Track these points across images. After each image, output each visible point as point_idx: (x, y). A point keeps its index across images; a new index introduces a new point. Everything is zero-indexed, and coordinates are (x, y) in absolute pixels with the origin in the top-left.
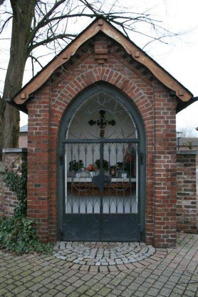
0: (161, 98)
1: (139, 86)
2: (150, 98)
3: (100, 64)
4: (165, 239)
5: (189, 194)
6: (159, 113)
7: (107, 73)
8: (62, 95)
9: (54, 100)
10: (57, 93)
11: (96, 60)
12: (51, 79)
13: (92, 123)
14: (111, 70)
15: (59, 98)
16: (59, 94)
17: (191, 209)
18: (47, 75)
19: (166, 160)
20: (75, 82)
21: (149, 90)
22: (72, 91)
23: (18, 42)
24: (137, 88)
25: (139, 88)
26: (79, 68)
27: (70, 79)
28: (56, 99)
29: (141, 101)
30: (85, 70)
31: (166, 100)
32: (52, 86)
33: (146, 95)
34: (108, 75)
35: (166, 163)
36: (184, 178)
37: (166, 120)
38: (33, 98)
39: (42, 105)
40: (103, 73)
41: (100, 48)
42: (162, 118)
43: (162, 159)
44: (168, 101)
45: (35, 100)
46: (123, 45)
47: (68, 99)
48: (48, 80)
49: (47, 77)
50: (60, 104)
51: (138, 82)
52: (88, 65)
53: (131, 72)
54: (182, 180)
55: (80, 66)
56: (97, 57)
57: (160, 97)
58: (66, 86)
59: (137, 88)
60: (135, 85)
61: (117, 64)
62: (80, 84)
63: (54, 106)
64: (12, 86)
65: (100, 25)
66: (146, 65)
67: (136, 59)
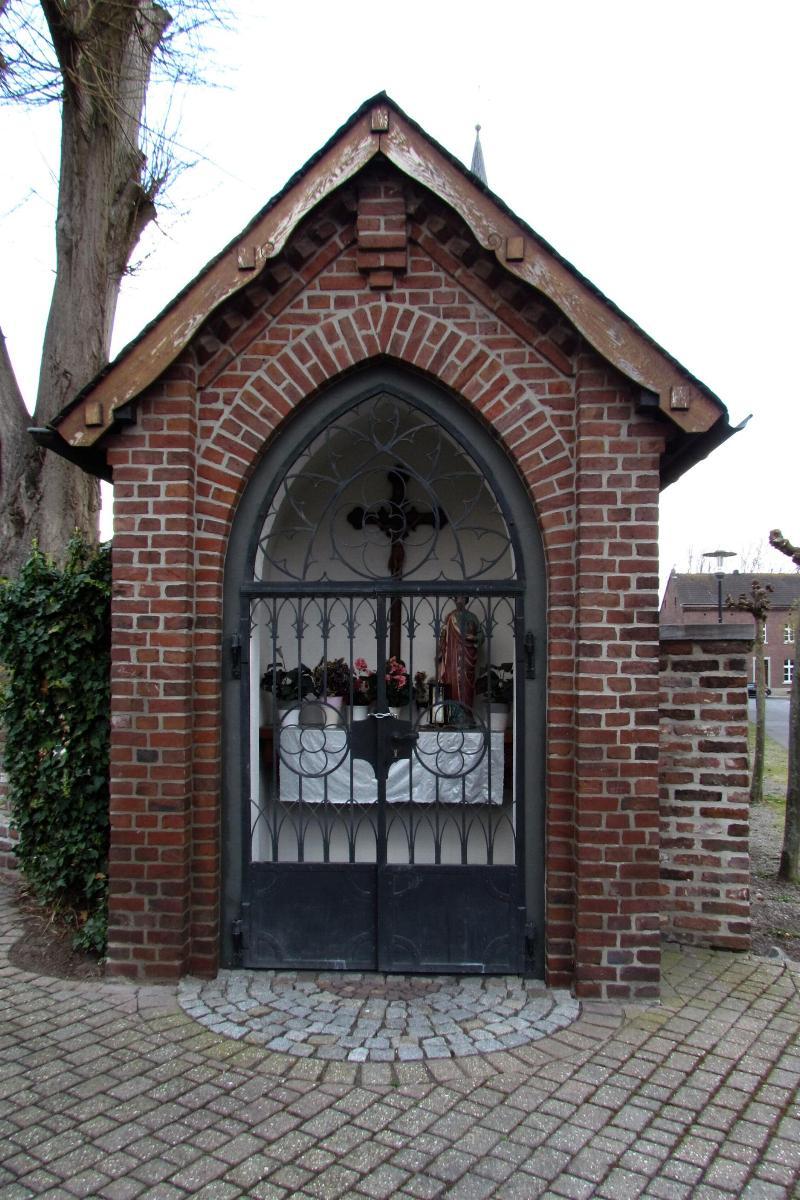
0: (605, 420)
1: (522, 374)
2: (562, 421)
3: (376, 289)
4: (619, 968)
5: (718, 797)
6: (596, 481)
7: (403, 326)
8: (238, 411)
9: (208, 431)
10: (219, 405)
11: (366, 273)
12: (196, 350)
13: (356, 519)
14: (418, 313)
15: (227, 425)
16: (228, 410)
17: (727, 855)
18: (182, 334)
19: (619, 662)
20: (285, 361)
21: (558, 389)
22: (274, 398)
24: (514, 381)
25: (524, 383)
26: (299, 305)
27: (269, 350)
28: (216, 426)
29: (529, 434)
30: (323, 312)
31: (624, 431)
32: (202, 376)
33: (548, 411)
34: (407, 335)
35: (620, 675)
36: (700, 733)
37: (620, 505)
38: (132, 423)
39: (165, 450)
40: (387, 327)
41: (380, 225)
42: (609, 498)
43: (604, 658)
44: (629, 434)
45: (138, 431)
46: (462, 210)
47: (260, 427)
48: (184, 355)
49: (180, 343)
50: (232, 447)
51: (520, 359)
52: (332, 294)
53: (493, 318)
54: (695, 741)
55: (304, 296)
56: (369, 261)
57: (599, 415)
58: (254, 375)
59: (514, 381)
60: (508, 370)
61: (444, 289)
62: (304, 369)
63: (209, 454)
65: (379, 133)
66: (548, 291)
67: (515, 270)
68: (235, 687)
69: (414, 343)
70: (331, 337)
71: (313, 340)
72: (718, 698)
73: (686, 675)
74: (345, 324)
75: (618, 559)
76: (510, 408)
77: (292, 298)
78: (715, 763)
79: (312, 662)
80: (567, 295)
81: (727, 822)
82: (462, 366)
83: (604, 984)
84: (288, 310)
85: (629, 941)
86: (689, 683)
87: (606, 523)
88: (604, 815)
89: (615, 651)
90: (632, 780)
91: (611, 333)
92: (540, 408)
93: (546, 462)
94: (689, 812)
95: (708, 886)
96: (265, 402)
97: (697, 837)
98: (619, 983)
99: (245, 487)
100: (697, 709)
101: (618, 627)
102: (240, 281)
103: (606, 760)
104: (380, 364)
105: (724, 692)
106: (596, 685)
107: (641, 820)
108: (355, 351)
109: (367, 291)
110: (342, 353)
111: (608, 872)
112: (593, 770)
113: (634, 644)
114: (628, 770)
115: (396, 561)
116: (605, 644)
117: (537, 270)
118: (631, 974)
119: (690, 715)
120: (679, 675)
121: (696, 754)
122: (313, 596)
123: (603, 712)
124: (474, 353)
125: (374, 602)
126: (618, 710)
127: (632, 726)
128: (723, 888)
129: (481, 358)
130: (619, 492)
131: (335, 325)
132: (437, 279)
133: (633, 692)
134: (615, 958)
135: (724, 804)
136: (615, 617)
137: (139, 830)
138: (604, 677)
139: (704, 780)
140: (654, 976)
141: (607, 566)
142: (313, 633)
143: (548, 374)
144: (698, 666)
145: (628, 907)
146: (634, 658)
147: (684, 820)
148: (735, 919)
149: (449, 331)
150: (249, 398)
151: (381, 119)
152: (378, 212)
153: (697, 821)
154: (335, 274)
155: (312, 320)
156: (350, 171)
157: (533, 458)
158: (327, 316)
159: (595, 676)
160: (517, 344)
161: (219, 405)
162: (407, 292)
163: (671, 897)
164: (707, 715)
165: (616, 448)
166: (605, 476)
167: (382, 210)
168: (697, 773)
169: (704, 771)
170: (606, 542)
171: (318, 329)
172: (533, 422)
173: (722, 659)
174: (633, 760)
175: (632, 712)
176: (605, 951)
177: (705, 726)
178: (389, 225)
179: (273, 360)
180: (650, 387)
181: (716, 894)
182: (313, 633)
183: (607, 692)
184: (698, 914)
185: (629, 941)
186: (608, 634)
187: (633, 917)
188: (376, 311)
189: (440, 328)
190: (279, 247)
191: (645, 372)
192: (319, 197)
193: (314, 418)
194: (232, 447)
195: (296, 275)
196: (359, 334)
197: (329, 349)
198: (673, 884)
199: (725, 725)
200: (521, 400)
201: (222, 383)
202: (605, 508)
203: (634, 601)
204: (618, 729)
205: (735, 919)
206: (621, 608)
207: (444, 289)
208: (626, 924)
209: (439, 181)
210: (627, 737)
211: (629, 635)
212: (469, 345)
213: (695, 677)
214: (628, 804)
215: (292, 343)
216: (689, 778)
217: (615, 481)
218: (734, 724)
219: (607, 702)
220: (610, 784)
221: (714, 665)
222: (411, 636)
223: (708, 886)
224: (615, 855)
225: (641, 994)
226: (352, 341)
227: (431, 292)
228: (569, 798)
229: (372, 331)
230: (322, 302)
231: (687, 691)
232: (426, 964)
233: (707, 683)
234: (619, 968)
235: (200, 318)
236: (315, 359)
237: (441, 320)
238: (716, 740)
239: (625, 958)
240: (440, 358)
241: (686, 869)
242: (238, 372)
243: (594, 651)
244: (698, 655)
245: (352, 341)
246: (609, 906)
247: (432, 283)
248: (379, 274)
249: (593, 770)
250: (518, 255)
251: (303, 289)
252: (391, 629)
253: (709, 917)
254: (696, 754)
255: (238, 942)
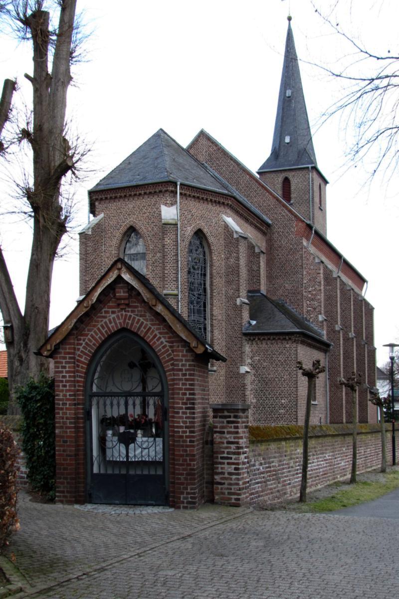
0: (180, 348)
1: (160, 333)
2: (171, 347)
3: (122, 309)
4: (185, 501)
5: (231, 458)
6: (178, 365)
7: (129, 320)
8: (87, 344)
9: (79, 349)
10: (82, 342)
11: (119, 305)
12: (75, 327)
13: (132, 365)
14: (133, 316)
15: (84, 347)
16: (84, 343)
17: (234, 477)
18: (71, 325)
19: (184, 416)
20: (99, 329)
21: (169, 338)
22: (95, 340)
23: (41, 248)
24: (159, 335)
25: (161, 336)
26: (102, 313)
27: (94, 326)
28: (81, 347)
29: (163, 350)
30: (108, 315)
31: (185, 351)
32: (77, 334)
33: (168, 344)
34: (130, 322)
35: (185, 420)
36: (226, 438)
37: (184, 372)
38: (59, 348)
39: (68, 356)
40: (125, 319)
41: (121, 293)
42: (181, 370)
43: (180, 415)
44: (186, 352)
45: (61, 350)
46: (140, 291)
47: (92, 348)
48: (72, 329)
49: (70, 327)
50: (85, 354)
51: (159, 329)
52: (110, 310)
53: (153, 317)
54: (225, 441)
55: (103, 310)
56: (119, 302)
57: (178, 347)
58: (91, 333)
59: (159, 335)
60: (157, 332)
61: (140, 309)
62: (104, 331)
63: (79, 356)
64: (37, 308)
65: (119, 269)
66: (163, 314)
67: (154, 308)
68: (88, 422)
69: (132, 324)
70: (110, 322)
71: (106, 323)
72: (231, 427)
73: (223, 420)
74: (114, 318)
75: (184, 387)
76: (157, 343)
77: (100, 311)
78: (230, 448)
79: (116, 415)
80: (167, 315)
81: (233, 466)
82: (145, 331)
83: (182, 505)
84: (99, 315)
85: (188, 493)
86: (223, 422)
87: (181, 377)
88: (181, 459)
89: (183, 413)
90: (188, 449)
91: (178, 326)
92: (165, 343)
93: (167, 359)
94: (224, 463)
95: (229, 487)
96: (93, 341)
97: (226, 471)
98: (185, 505)
99: (89, 365)
100: (226, 430)
101: (184, 406)
102: (85, 310)
103: (181, 443)
104: (123, 330)
105: (233, 425)
106: (179, 422)
107: (191, 460)
108: (117, 327)
109: (119, 309)
110: (113, 327)
111: (182, 474)
112: (178, 446)
113: (188, 411)
114: (187, 446)
115: (144, 382)
116: (181, 411)
117: (160, 308)
118: (189, 503)
119: (224, 433)
120: (221, 420)
121: (225, 445)
122: (108, 396)
123: (180, 430)
124: (148, 327)
125: (124, 398)
126: (184, 429)
127: (188, 434)
128: (233, 487)
129: (150, 328)
130: (184, 368)
131: (111, 319)
132: (138, 306)
133: (188, 424)
134: (184, 498)
135: (233, 461)
136: (183, 403)
137: (63, 462)
138: (181, 420)
139: (228, 453)
140: (194, 503)
141: (180, 389)
142: (115, 407)
143: (167, 333)
144: (226, 417)
145: (188, 484)
146: (188, 415)
147: (223, 466)
148: (236, 497)
149: (141, 322)
150: (89, 340)
151: (119, 265)
152: (120, 289)
153: (226, 466)
154: (111, 304)
155: (105, 317)
156: (112, 279)
157: (164, 357)
158: (109, 316)
159: (178, 420)
160: (159, 325)
161: (82, 342)
162: (130, 309)
163: (219, 491)
164: (229, 433)
165: (183, 356)
166: (180, 364)
167: (121, 288)
168: (226, 451)
169: (227, 450)
170: (181, 382)
171: (107, 320)
172: (164, 347)
173: (232, 415)
174: (188, 443)
175: (188, 430)
176: (182, 496)
177: (228, 436)
178: (124, 292)
179: (95, 329)
180: (188, 341)
181: (231, 489)
182: (115, 407)
183: (182, 424)
184: (227, 496)
185: (188, 493)
186: (182, 408)
187: (189, 487)
188: (122, 315)
189: (139, 320)
190: (94, 301)
191: (186, 337)
192: (104, 287)
193: (103, 350)
194: (85, 354)
195: (101, 305)
196: (118, 321)
197: (110, 326)
198: (220, 487)
199: (233, 436)
200: (160, 341)
201: (82, 335)
202: (180, 373)
203: (188, 399)
204: (184, 435)
205: (236, 497)
206: (185, 401)
207: (140, 309)
208: (187, 489)
209: (135, 283)
210: (187, 437)
211: (187, 408)
212: (147, 325)
213: (225, 420)
214: (187, 455)
215: (100, 324)
216: (223, 452)
217: (183, 365)
218: (235, 435)
219: (181, 427)
220: (182, 450)
221: (230, 417)
222: (148, 408)
223: (229, 487)
224: (184, 470)
225: (191, 508)
226: (116, 324)
227: (136, 309)
228: (173, 454)
229: (121, 321)
230: (107, 312)
231: (223, 425)
232: (139, 502)
233: (228, 422)
234: (185, 501)
235: (75, 320)
236: (106, 329)
237: (139, 318)
238: (231, 440)
239: (186, 498)
240: (139, 328)
241: (223, 481)
242: (86, 332)
243: (178, 413)
244: (226, 414)
245: (116, 324)
246: (182, 484)
247: (136, 307)
248: (122, 305)
249: (178, 446)
250: (154, 304)
251: (102, 309)
252: (144, 405)
253: (229, 496)
254: (225, 445)
255: (90, 495)
